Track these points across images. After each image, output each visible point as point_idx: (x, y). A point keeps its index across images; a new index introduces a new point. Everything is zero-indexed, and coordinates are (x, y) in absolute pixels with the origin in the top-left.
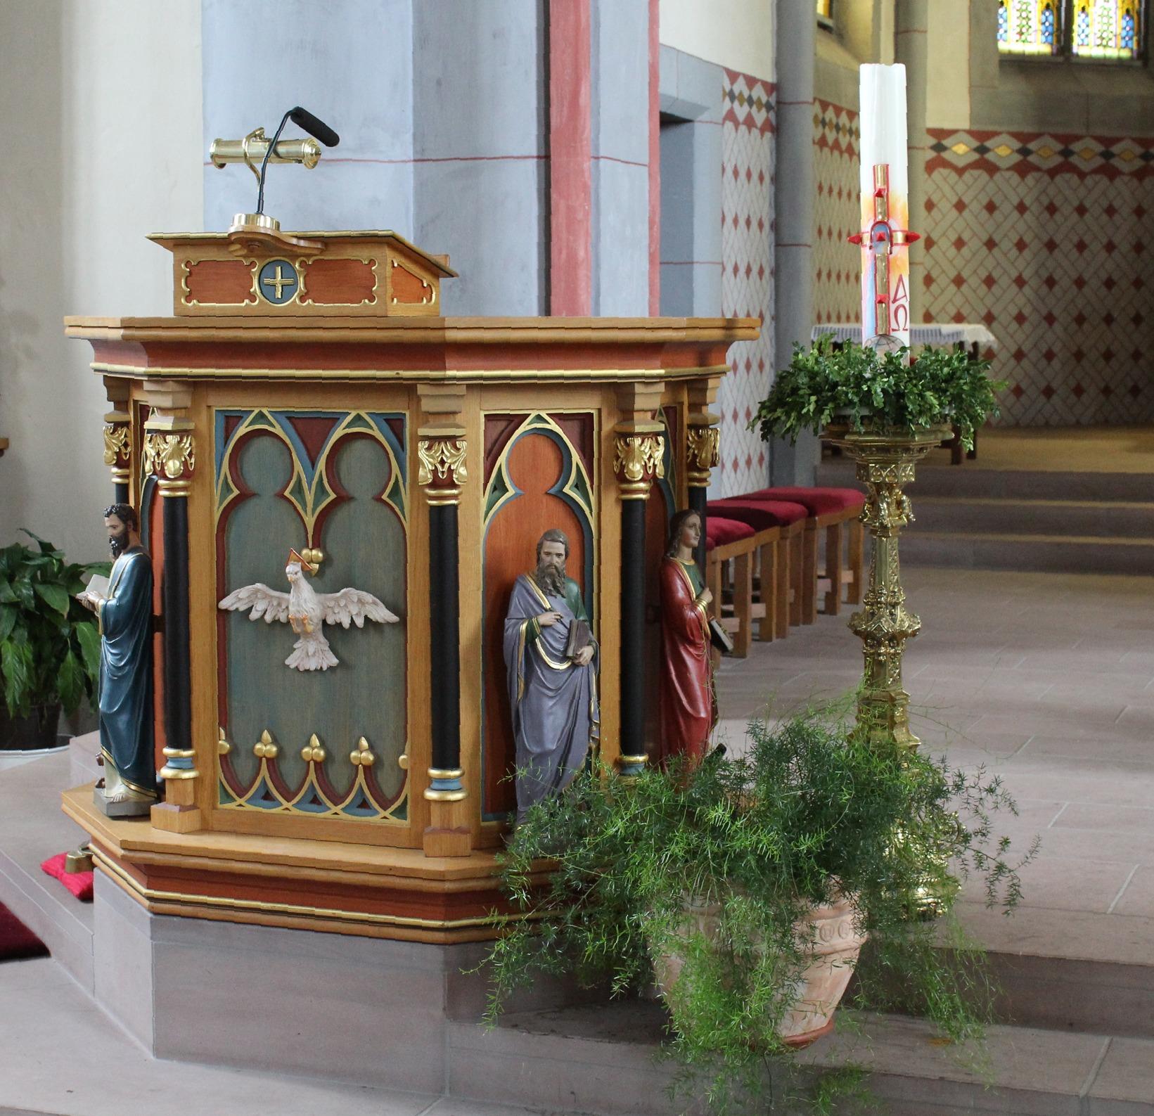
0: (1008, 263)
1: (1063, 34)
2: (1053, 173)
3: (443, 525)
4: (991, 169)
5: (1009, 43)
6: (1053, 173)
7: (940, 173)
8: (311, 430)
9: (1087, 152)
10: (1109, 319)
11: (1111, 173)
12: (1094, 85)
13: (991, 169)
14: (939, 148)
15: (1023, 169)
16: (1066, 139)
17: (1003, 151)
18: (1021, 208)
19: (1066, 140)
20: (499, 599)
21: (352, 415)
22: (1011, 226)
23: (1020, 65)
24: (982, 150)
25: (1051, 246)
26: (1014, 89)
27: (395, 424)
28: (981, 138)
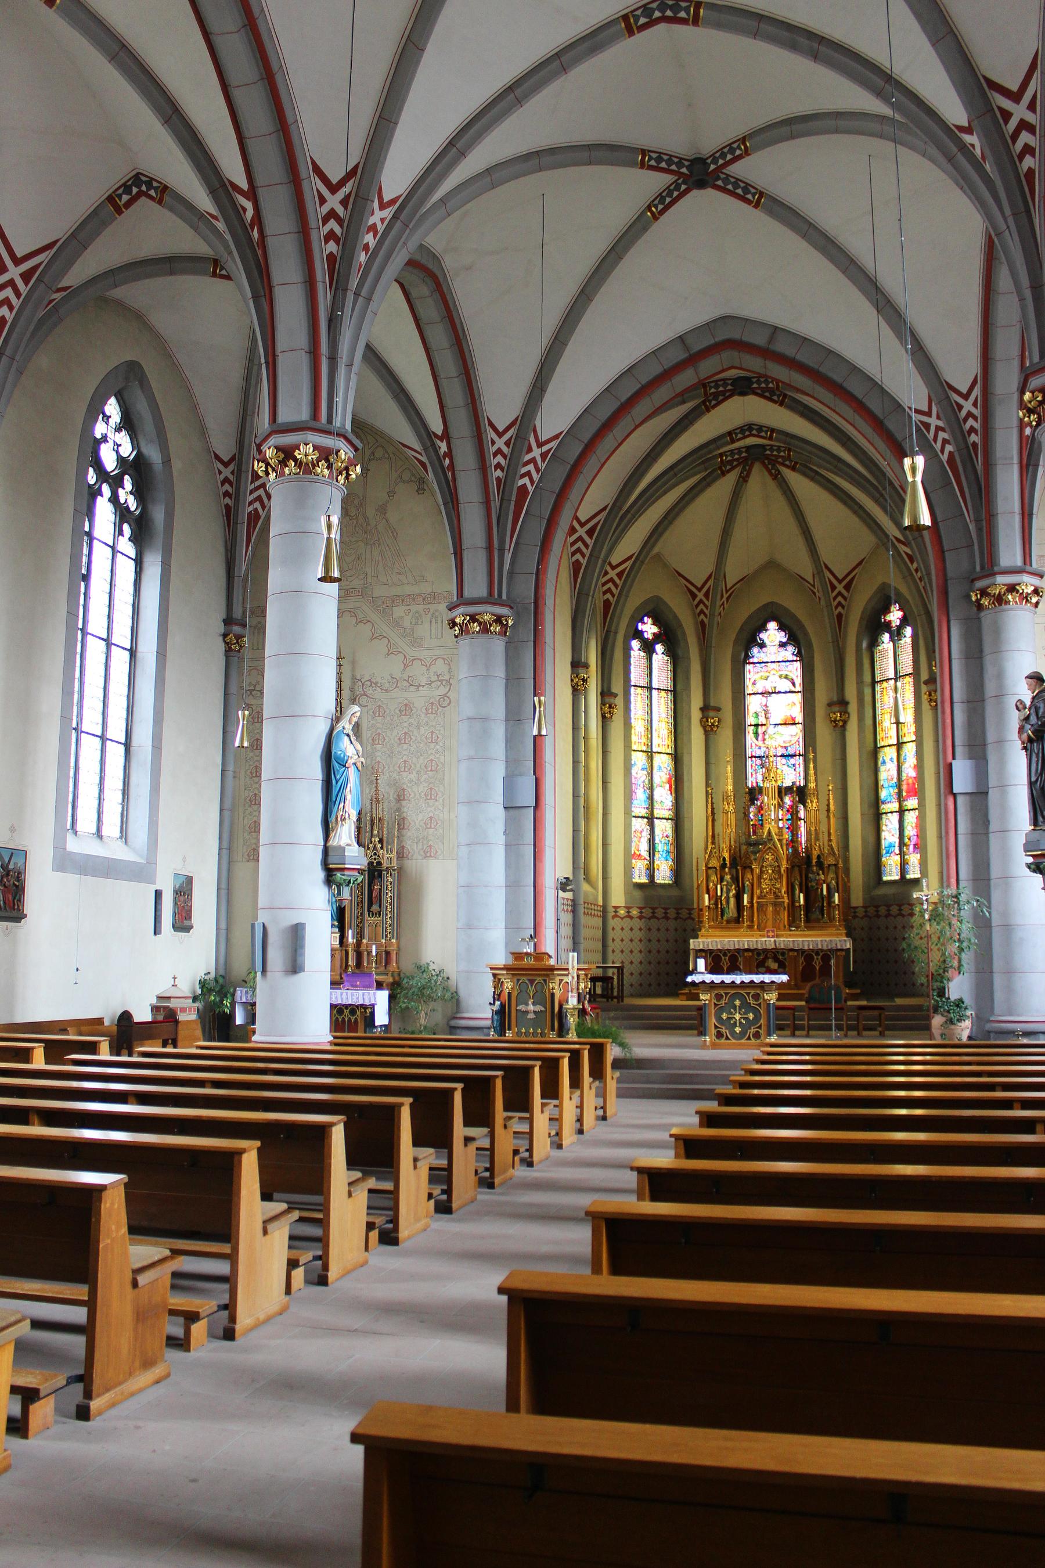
0: (637, 946)
1: (651, 876)
2: (649, 919)
3: (553, 995)
4: (631, 918)
5: (636, 880)
6: (649, 919)
7: (616, 919)
8: (532, 982)
9: (660, 913)
10: (668, 963)
11: (667, 918)
12: (662, 892)
13: (631, 918)
14: (616, 912)
15: (640, 918)
16: (653, 909)
17: (635, 912)
18: (640, 929)
19: (653, 909)
20: (561, 1006)
21: (539, 979)
22: (638, 935)
23: (640, 886)
24: (628, 912)
25: (650, 940)
26: (637, 894)
27: (545, 981)
28: (628, 908)
